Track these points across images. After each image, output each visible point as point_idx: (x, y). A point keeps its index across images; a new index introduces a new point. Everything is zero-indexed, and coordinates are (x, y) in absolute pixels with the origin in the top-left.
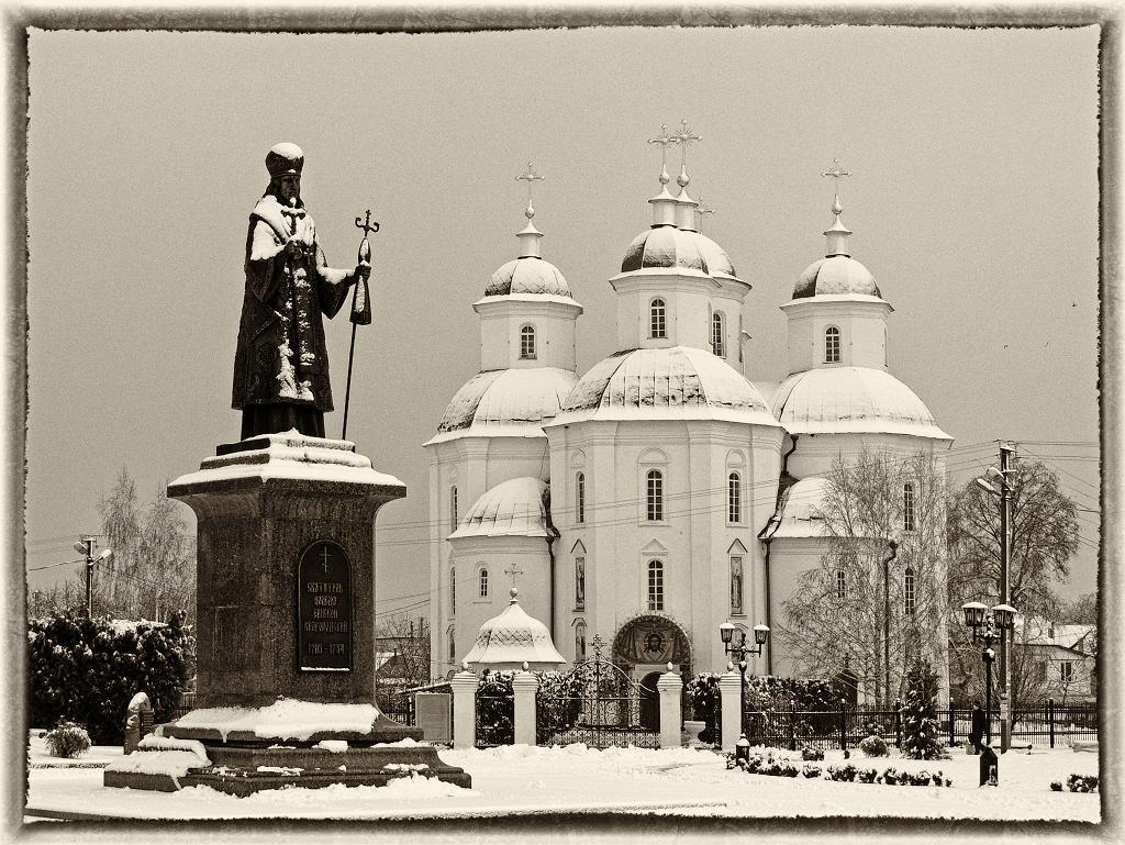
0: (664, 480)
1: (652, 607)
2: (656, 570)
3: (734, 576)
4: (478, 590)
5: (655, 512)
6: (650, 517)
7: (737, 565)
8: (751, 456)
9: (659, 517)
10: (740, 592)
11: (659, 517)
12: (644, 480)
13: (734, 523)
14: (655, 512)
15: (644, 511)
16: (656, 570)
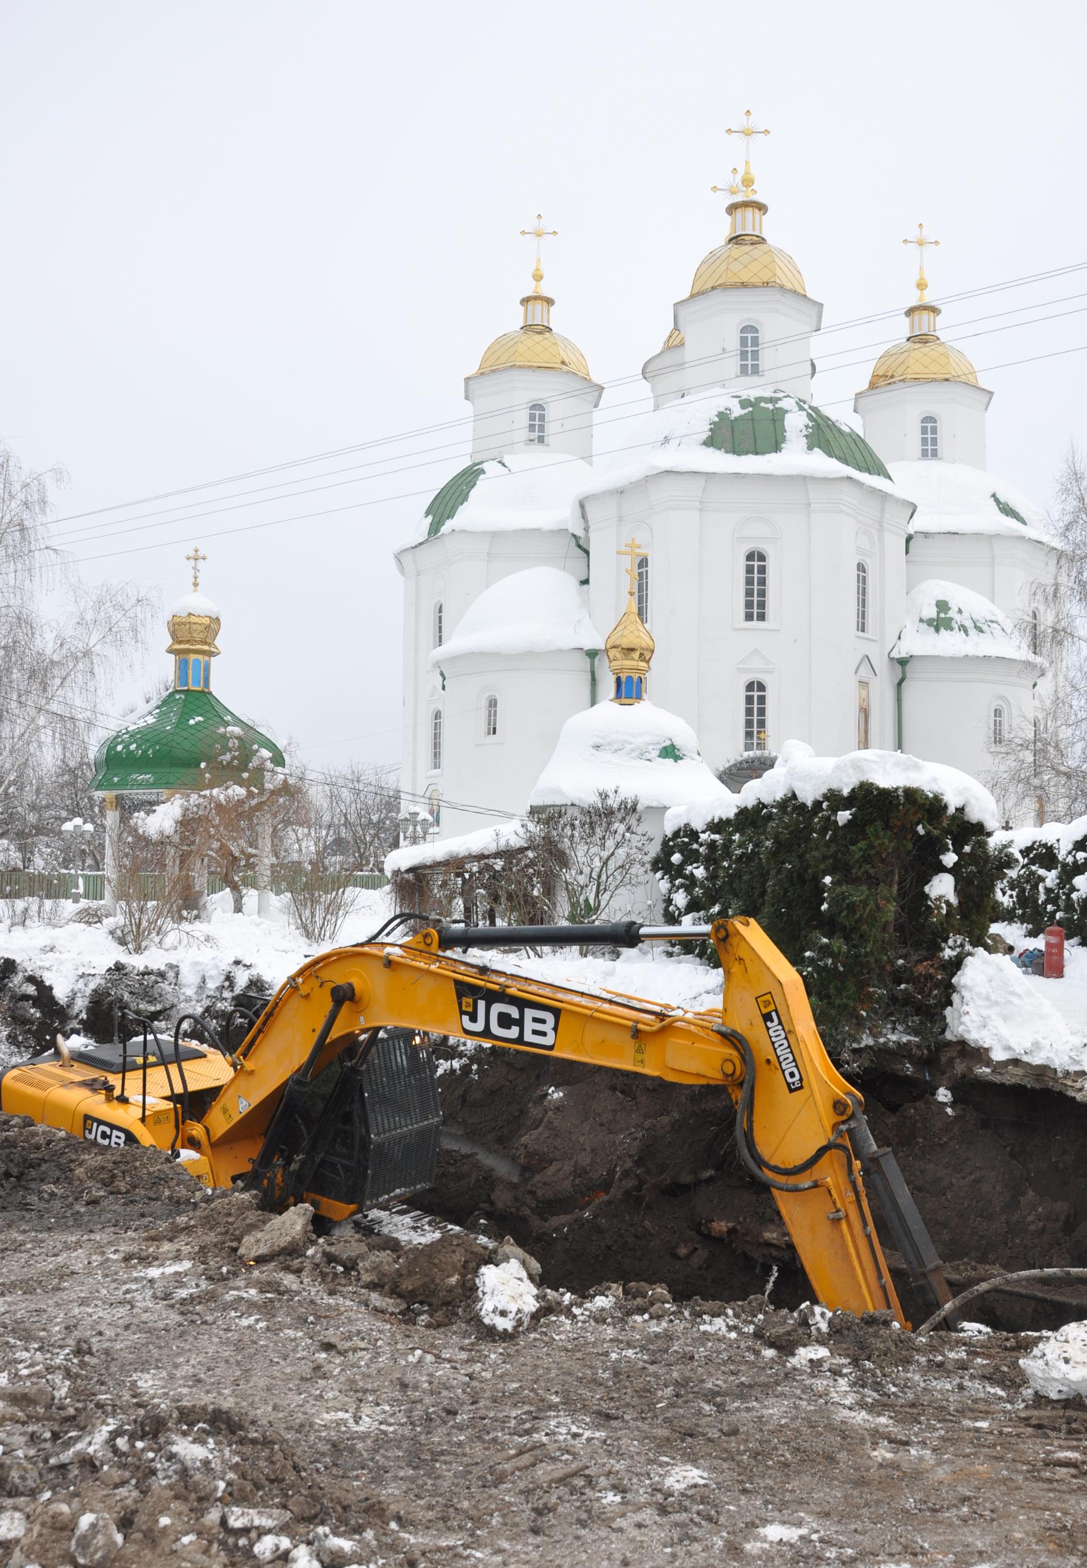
0: (771, 565)
1: (748, 747)
2: (756, 694)
3: (861, 708)
4: (483, 726)
5: (756, 607)
6: (749, 617)
7: (864, 693)
8: (881, 540)
9: (762, 617)
10: (866, 732)
11: (762, 617)
12: (742, 563)
13: (862, 634)
14: (756, 607)
15: (741, 611)
16: (756, 694)
